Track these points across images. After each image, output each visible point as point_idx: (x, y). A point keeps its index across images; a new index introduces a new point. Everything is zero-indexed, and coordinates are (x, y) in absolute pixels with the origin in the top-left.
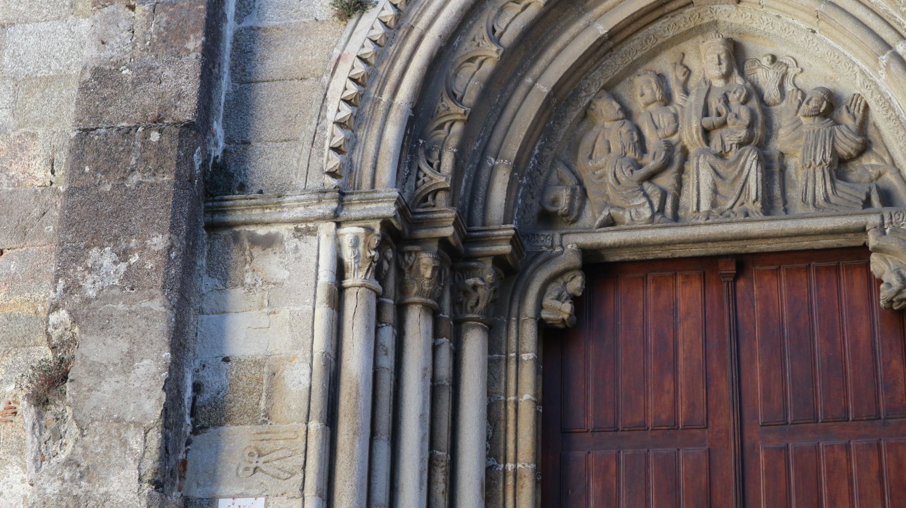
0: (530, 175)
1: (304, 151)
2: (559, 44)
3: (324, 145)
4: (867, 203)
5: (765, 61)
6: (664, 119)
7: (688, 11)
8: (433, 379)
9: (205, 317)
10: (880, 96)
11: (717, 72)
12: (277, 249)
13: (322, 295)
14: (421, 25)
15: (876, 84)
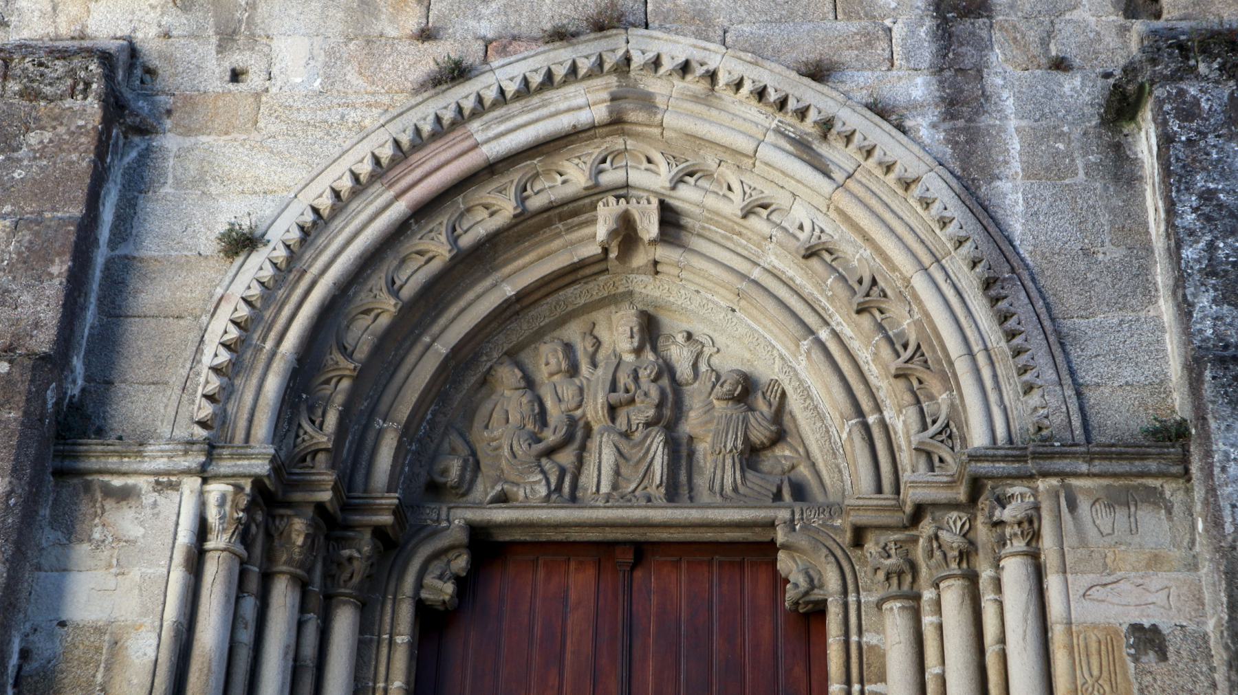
0: (420, 441)
1: (174, 397)
2: (462, 303)
3: (196, 392)
4: (778, 496)
5: (680, 338)
6: (568, 392)
7: (602, 278)
8: (296, 659)
9: (43, 574)
12: (133, 503)
13: (179, 556)
14: (315, 270)
15: (795, 370)
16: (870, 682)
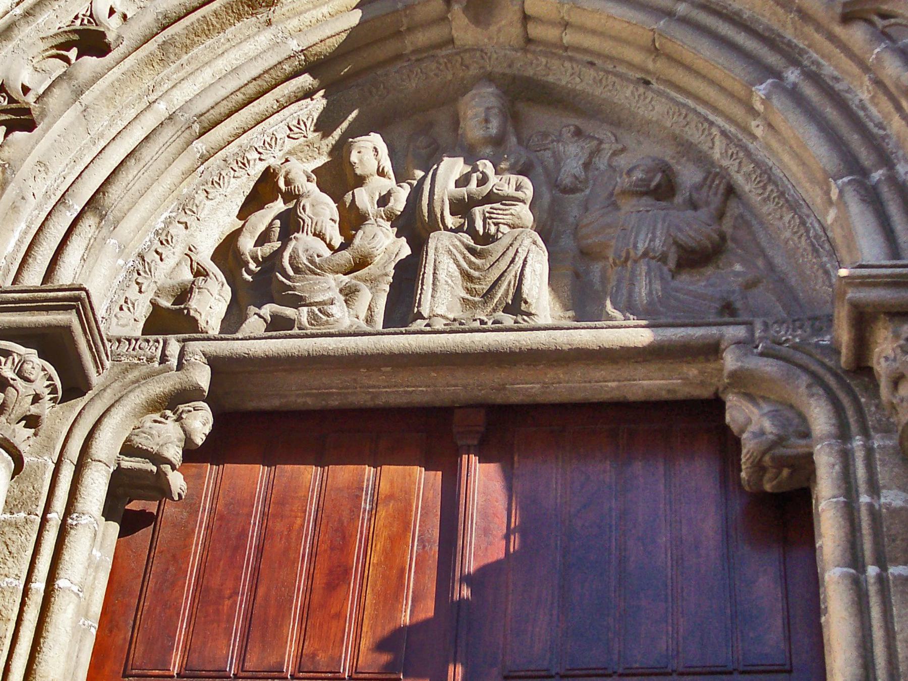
10: (753, 165)
11: (482, 132)
16: (896, 562)
